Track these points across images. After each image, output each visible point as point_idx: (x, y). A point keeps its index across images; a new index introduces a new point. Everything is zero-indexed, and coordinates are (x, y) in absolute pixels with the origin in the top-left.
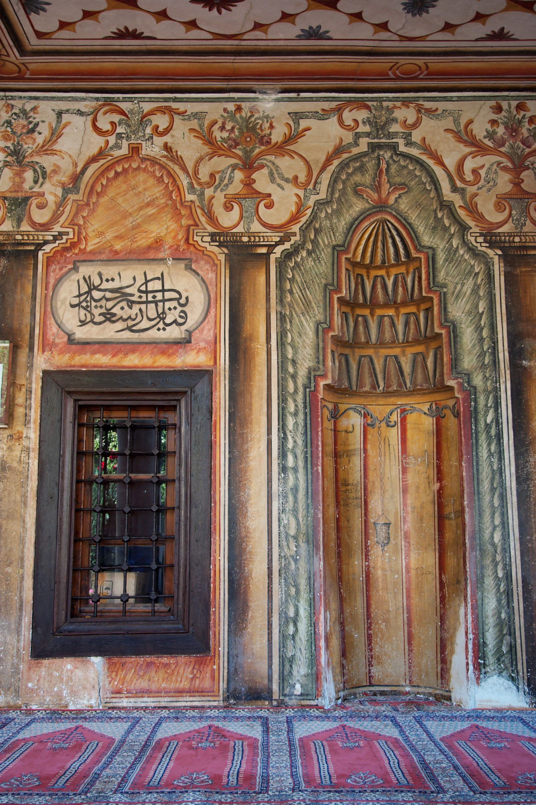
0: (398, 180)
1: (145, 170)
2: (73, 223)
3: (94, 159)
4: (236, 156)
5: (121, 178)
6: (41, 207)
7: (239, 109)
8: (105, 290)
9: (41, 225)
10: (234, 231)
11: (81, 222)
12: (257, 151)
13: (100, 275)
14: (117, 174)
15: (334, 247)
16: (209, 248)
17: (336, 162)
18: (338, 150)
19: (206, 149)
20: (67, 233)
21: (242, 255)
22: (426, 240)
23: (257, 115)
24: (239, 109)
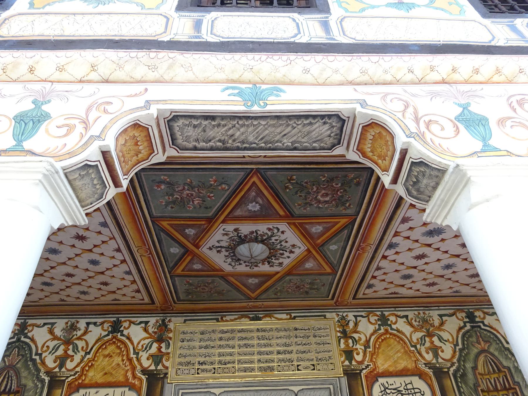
0: (486, 339)
1: (392, 338)
2: (371, 361)
3: (372, 335)
4: (424, 332)
5: (384, 342)
6: (358, 354)
7: (419, 313)
8: (391, 389)
9: (360, 362)
10: (433, 362)
11: (374, 360)
12: (431, 329)
13: (387, 382)
14: (383, 340)
15: (472, 368)
16: (426, 370)
17: (461, 333)
18: (460, 328)
19: (412, 329)
20: (370, 365)
21: (440, 373)
22: (505, 363)
23: (426, 316)
24: (419, 313)
